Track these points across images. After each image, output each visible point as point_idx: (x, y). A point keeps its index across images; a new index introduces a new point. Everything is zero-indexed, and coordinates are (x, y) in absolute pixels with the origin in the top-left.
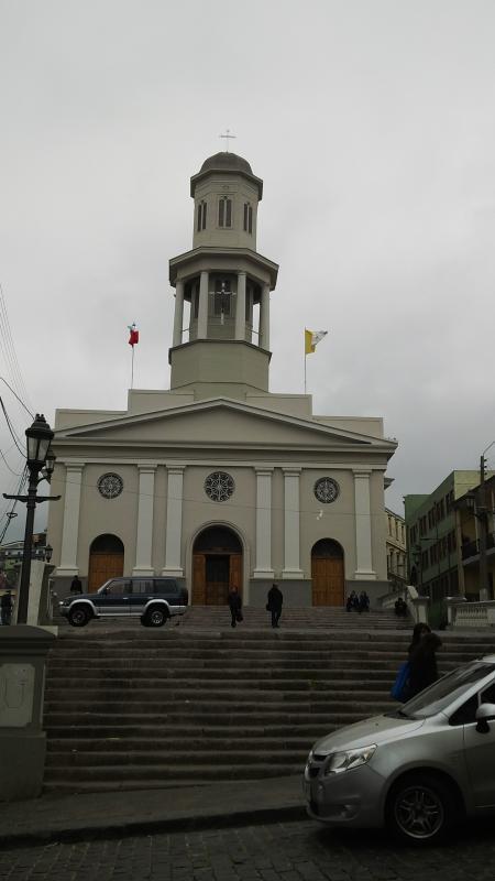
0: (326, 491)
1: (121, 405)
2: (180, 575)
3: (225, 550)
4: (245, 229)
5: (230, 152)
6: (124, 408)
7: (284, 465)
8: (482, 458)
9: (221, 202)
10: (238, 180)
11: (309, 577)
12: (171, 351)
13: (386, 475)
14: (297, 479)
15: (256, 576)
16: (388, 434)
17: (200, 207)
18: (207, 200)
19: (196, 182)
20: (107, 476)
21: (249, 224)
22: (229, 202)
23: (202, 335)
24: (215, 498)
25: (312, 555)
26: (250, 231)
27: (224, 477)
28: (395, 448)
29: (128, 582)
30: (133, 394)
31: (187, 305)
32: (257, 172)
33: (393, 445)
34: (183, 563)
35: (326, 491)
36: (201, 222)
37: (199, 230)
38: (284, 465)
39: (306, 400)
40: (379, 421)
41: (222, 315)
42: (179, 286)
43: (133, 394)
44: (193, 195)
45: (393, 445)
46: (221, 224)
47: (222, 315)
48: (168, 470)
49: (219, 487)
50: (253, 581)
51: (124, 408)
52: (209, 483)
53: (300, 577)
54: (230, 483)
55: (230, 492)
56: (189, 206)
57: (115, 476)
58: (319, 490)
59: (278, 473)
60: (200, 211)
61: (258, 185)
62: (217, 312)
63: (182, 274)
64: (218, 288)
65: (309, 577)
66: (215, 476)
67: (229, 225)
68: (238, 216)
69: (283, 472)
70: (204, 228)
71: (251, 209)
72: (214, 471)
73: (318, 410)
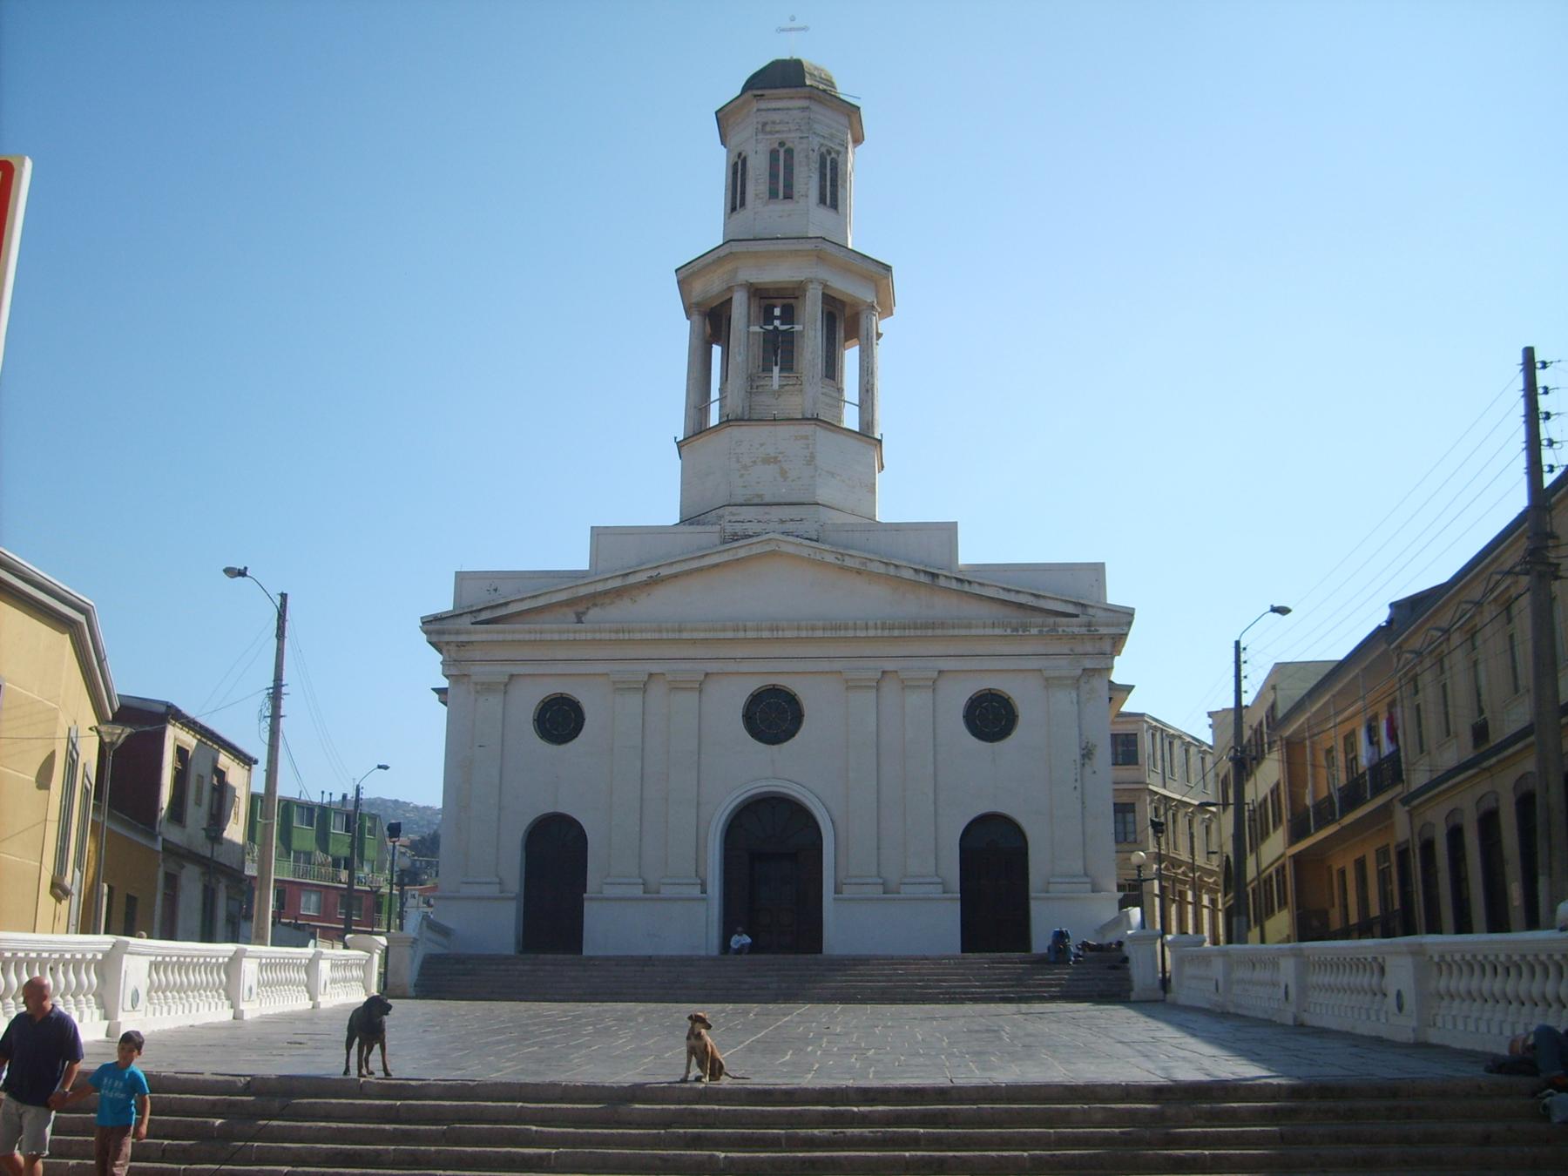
1: (577, 558)
4: (822, 200)
5: (795, 57)
6: (581, 562)
8: (1237, 643)
9: (774, 154)
12: (680, 445)
13: (1118, 677)
16: (1115, 596)
17: (736, 164)
19: (725, 118)
21: (831, 192)
23: (736, 404)
26: (834, 206)
28: (1130, 624)
29: (425, 923)
30: (598, 534)
31: (717, 351)
32: (844, 90)
33: (1125, 617)
36: (737, 199)
37: (733, 209)
39: (948, 531)
40: (1097, 570)
41: (776, 370)
43: (598, 534)
44: (723, 143)
45: (1125, 617)
46: (773, 194)
47: (776, 370)
51: (586, 567)
56: (717, 161)
60: (735, 173)
61: (851, 112)
64: (769, 318)
67: (788, 196)
68: (807, 181)
70: (743, 204)
71: (835, 168)
72: (755, 684)
73: (971, 553)
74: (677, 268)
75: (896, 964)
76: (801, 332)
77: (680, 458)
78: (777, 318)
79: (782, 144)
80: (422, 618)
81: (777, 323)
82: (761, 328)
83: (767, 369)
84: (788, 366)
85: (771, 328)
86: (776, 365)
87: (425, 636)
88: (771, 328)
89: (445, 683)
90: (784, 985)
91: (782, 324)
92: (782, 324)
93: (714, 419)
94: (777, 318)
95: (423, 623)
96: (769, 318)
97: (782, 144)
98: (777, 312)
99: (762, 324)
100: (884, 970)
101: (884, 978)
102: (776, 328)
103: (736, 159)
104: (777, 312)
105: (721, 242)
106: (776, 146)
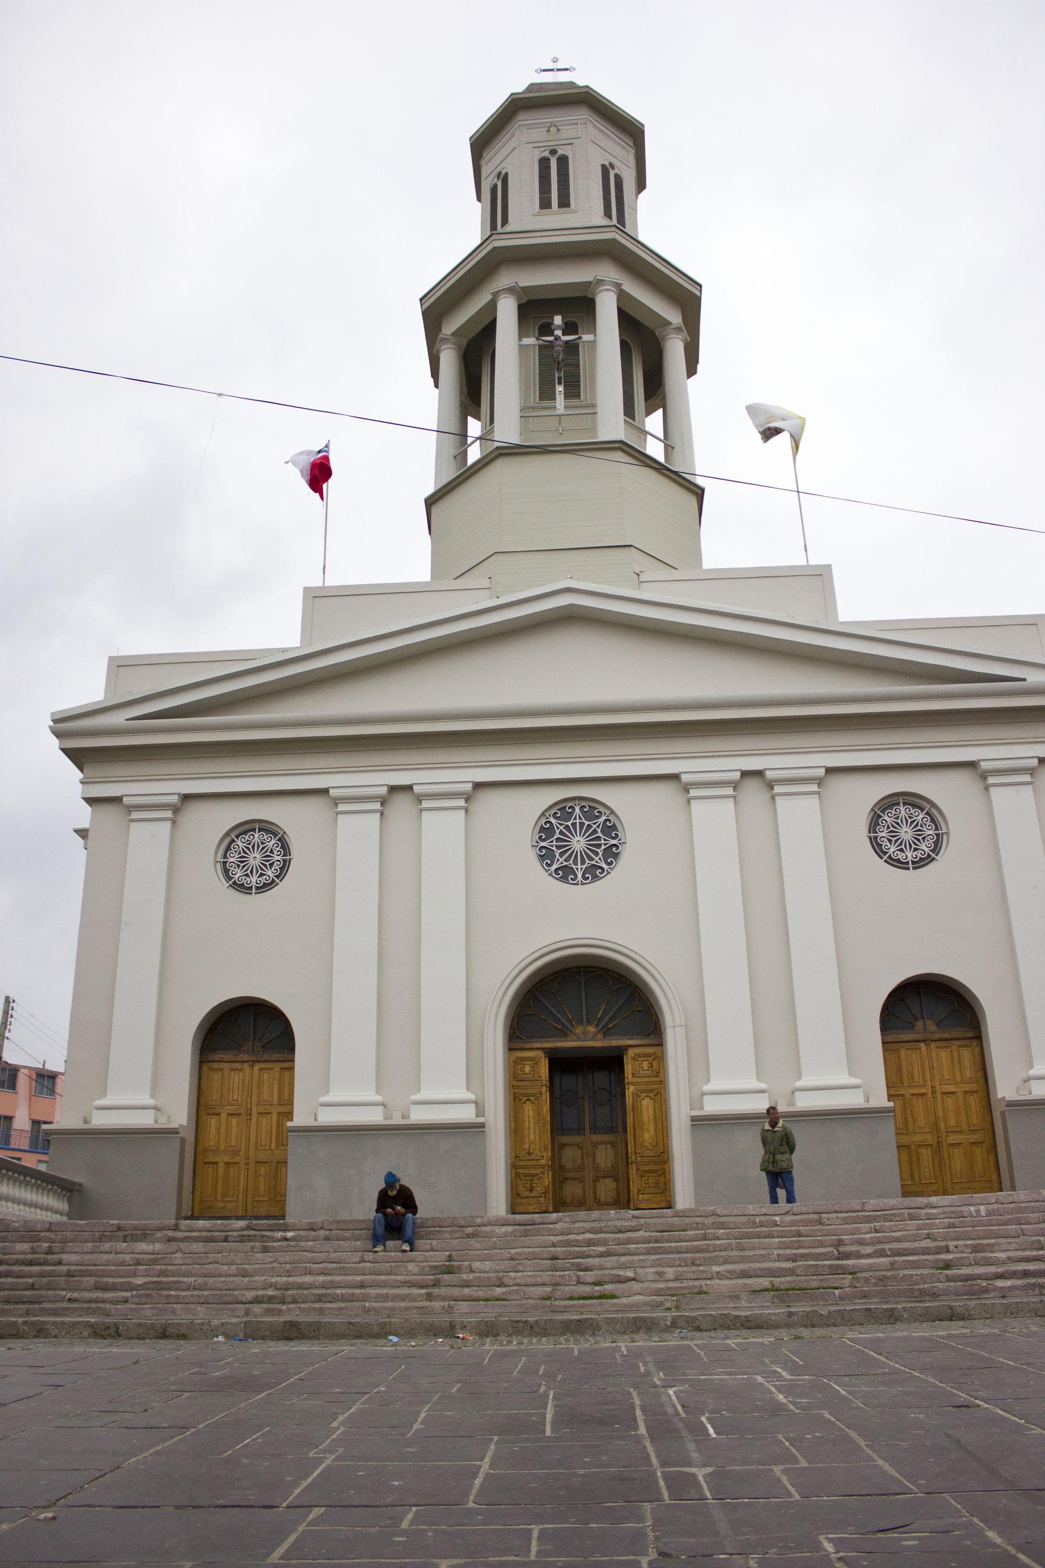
0: (906, 833)
2: (466, 1114)
3: (606, 1033)
7: (773, 764)
9: (544, 164)
10: (582, 114)
11: (880, 1099)
14: (814, 801)
15: (712, 1106)
18: (508, 167)
20: (246, 828)
22: (563, 161)
24: (565, 874)
25: (882, 1030)
27: (592, 809)
34: (473, 1075)
35: (906, 833)
38: (773, 764)
41: (560, 388)
42: (449, 358)
48: (419, 798)
49: (579, 843)
50: (700, 1123)
52: (546, 831)
53: (854, 1100)
54: (610, 829)
55: (612, 854)
57: (267, 828)
58: (883, 833)
59: (753, 790)
62: (547, 394)
63: (451, 326)
65: (880, 1099)
66: (563, 810)
67: (564, 202)
69: (770, 785)
74: (421, 296)
75: (875, 1219)
76: (593, 343)
77: (430, 533)
78: (558, 328)
79: (553, 152)
80: (52, 714)
81: (558, 333)
82: (537, 339)
83: (547, 394)
84: (573, 390)
85: (551, 338)
86: (560, 383)
87: (55, 742)
88: (551, 338)
89: (84, 815)
90: (670, 1272)
91: (564, 334)
92: (564, 334)
93: (474, 454)
94: (558, 328)
95: (55, 721)
96: (546, 329)
97: (553, 152)
98: (558, 320)
99: (537, 335)
100: (858, 1231)
101: (869, 1250)
102: (557, 338)
103: (496, 179)
104: (558, 320)
105: (479, 242)
106: (546, 154)
